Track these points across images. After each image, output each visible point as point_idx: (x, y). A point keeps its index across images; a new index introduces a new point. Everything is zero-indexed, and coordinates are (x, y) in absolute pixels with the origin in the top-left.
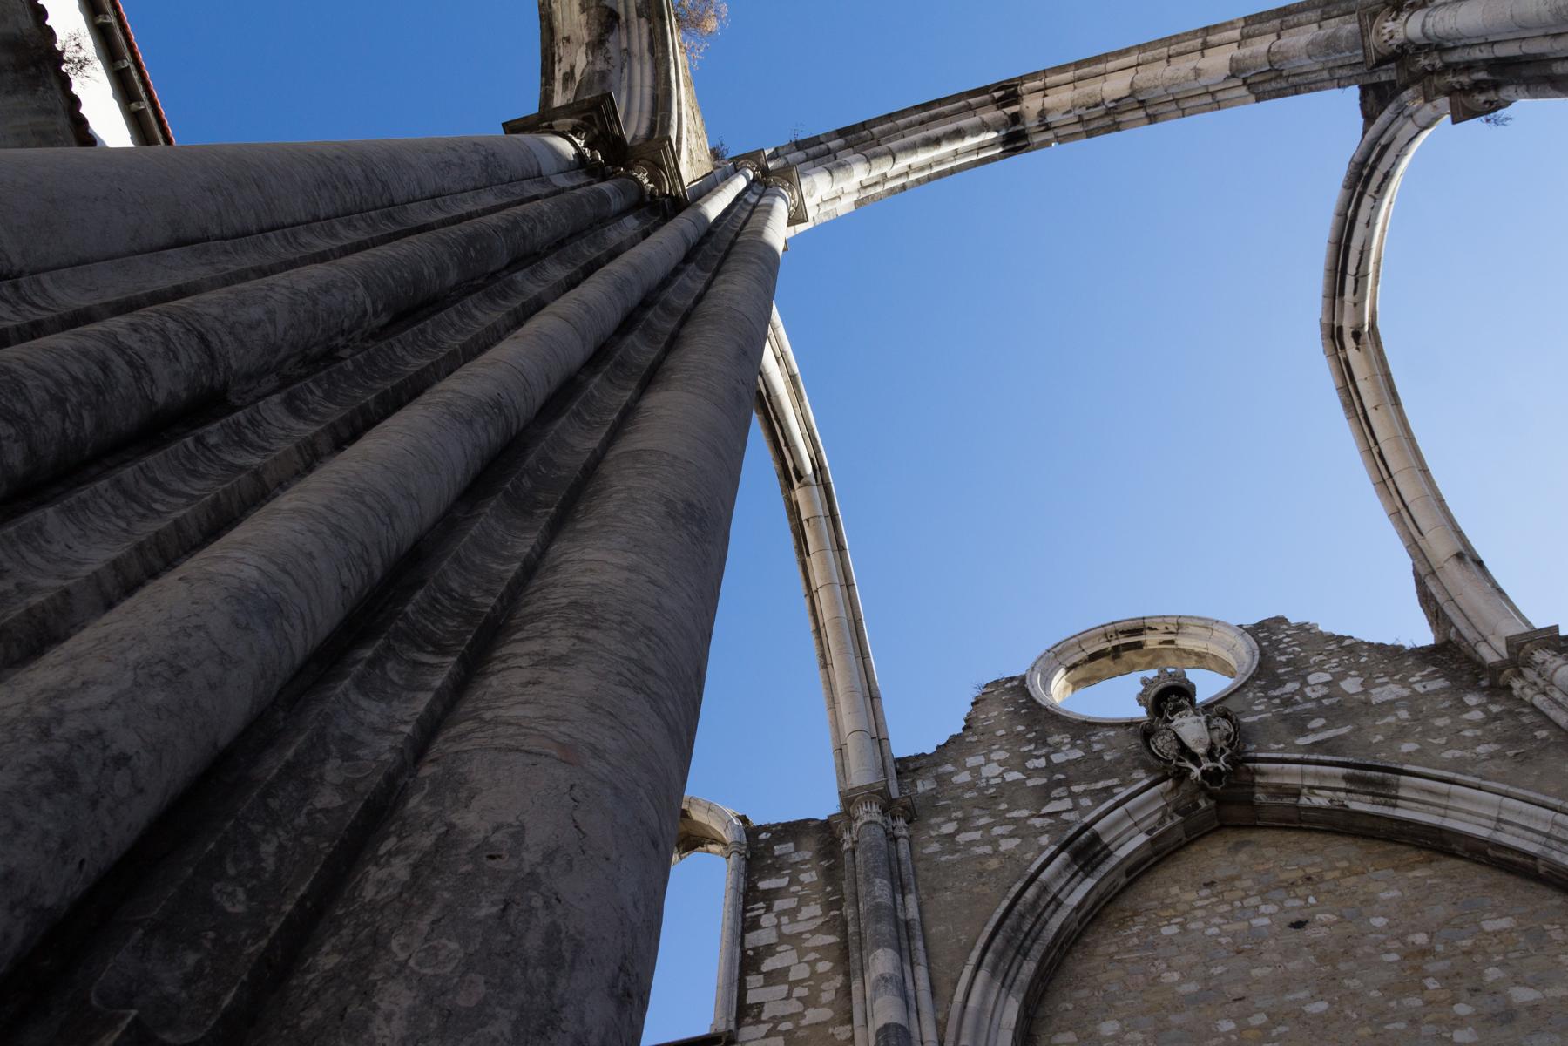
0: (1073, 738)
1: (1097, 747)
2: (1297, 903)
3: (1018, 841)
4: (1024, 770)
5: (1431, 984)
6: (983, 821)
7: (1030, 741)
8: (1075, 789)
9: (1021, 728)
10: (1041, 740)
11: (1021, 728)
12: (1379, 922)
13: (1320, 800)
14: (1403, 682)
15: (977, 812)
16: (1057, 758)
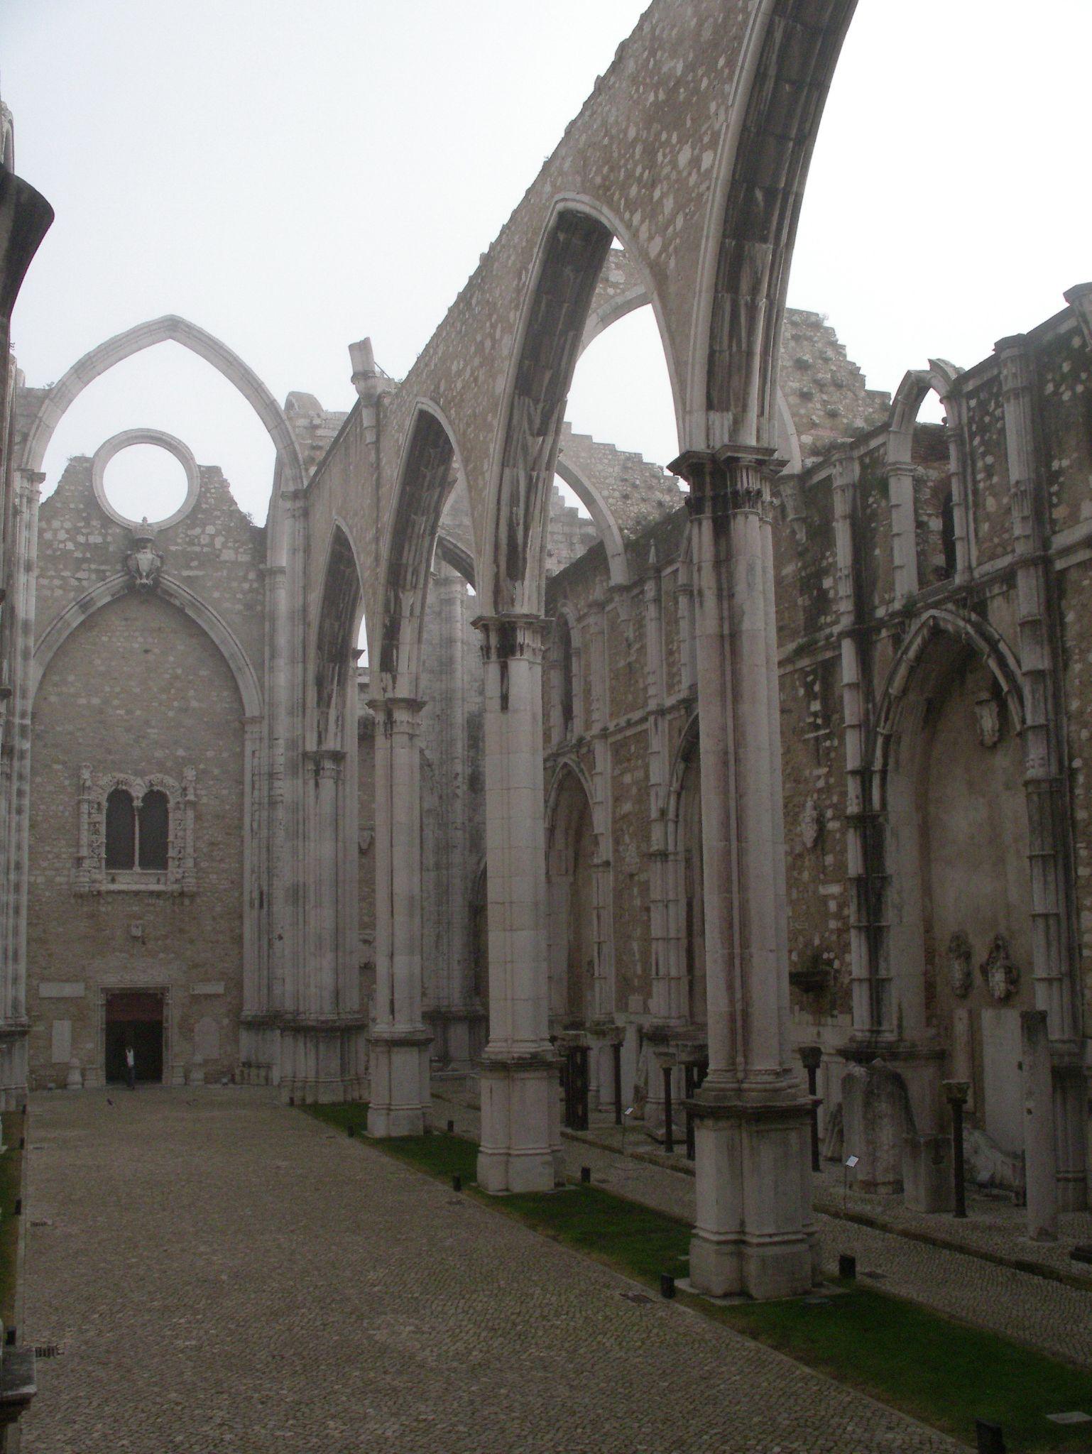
0: (103, 526)
1: (109, 539)
2: (150, 640)
3: (61, 592)
4: (77, 544)
5: (173, 691)
6: (52, 573)
7: (84, 518)
8: (93, 567)
9: (82, 506)
10: (87, 520)
11: (82, 506)
12: (172, 659)
13: (177, 603)
14: (236, 551)
15: (50, 566)
16: (92, 539)
